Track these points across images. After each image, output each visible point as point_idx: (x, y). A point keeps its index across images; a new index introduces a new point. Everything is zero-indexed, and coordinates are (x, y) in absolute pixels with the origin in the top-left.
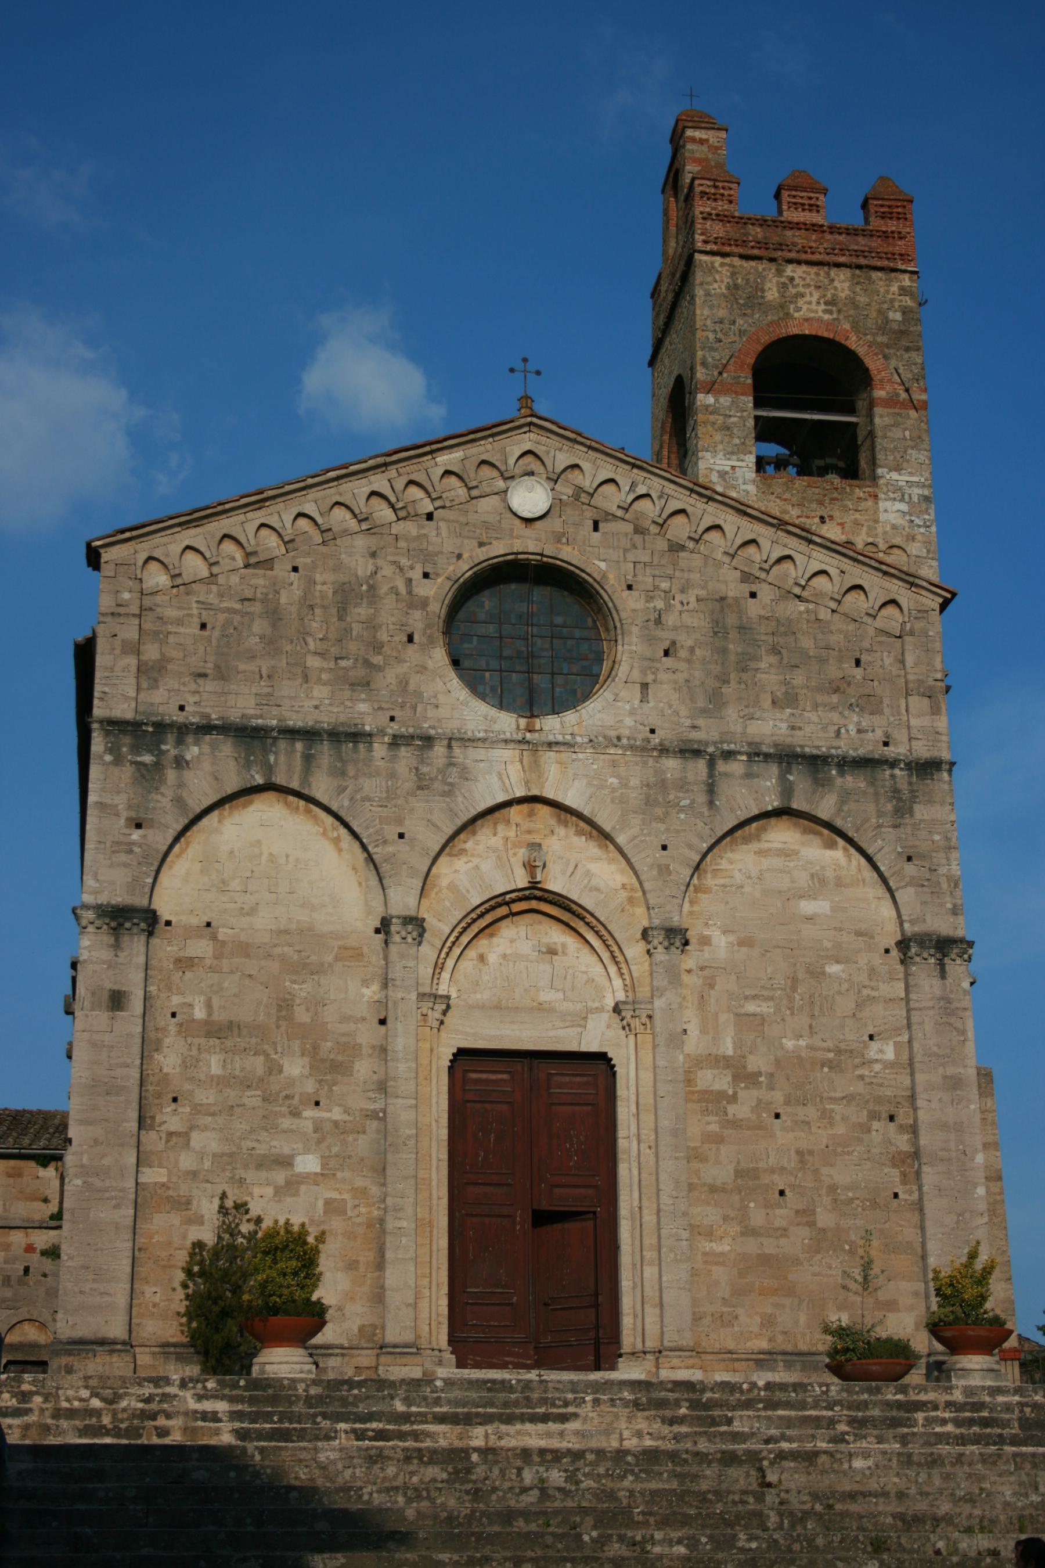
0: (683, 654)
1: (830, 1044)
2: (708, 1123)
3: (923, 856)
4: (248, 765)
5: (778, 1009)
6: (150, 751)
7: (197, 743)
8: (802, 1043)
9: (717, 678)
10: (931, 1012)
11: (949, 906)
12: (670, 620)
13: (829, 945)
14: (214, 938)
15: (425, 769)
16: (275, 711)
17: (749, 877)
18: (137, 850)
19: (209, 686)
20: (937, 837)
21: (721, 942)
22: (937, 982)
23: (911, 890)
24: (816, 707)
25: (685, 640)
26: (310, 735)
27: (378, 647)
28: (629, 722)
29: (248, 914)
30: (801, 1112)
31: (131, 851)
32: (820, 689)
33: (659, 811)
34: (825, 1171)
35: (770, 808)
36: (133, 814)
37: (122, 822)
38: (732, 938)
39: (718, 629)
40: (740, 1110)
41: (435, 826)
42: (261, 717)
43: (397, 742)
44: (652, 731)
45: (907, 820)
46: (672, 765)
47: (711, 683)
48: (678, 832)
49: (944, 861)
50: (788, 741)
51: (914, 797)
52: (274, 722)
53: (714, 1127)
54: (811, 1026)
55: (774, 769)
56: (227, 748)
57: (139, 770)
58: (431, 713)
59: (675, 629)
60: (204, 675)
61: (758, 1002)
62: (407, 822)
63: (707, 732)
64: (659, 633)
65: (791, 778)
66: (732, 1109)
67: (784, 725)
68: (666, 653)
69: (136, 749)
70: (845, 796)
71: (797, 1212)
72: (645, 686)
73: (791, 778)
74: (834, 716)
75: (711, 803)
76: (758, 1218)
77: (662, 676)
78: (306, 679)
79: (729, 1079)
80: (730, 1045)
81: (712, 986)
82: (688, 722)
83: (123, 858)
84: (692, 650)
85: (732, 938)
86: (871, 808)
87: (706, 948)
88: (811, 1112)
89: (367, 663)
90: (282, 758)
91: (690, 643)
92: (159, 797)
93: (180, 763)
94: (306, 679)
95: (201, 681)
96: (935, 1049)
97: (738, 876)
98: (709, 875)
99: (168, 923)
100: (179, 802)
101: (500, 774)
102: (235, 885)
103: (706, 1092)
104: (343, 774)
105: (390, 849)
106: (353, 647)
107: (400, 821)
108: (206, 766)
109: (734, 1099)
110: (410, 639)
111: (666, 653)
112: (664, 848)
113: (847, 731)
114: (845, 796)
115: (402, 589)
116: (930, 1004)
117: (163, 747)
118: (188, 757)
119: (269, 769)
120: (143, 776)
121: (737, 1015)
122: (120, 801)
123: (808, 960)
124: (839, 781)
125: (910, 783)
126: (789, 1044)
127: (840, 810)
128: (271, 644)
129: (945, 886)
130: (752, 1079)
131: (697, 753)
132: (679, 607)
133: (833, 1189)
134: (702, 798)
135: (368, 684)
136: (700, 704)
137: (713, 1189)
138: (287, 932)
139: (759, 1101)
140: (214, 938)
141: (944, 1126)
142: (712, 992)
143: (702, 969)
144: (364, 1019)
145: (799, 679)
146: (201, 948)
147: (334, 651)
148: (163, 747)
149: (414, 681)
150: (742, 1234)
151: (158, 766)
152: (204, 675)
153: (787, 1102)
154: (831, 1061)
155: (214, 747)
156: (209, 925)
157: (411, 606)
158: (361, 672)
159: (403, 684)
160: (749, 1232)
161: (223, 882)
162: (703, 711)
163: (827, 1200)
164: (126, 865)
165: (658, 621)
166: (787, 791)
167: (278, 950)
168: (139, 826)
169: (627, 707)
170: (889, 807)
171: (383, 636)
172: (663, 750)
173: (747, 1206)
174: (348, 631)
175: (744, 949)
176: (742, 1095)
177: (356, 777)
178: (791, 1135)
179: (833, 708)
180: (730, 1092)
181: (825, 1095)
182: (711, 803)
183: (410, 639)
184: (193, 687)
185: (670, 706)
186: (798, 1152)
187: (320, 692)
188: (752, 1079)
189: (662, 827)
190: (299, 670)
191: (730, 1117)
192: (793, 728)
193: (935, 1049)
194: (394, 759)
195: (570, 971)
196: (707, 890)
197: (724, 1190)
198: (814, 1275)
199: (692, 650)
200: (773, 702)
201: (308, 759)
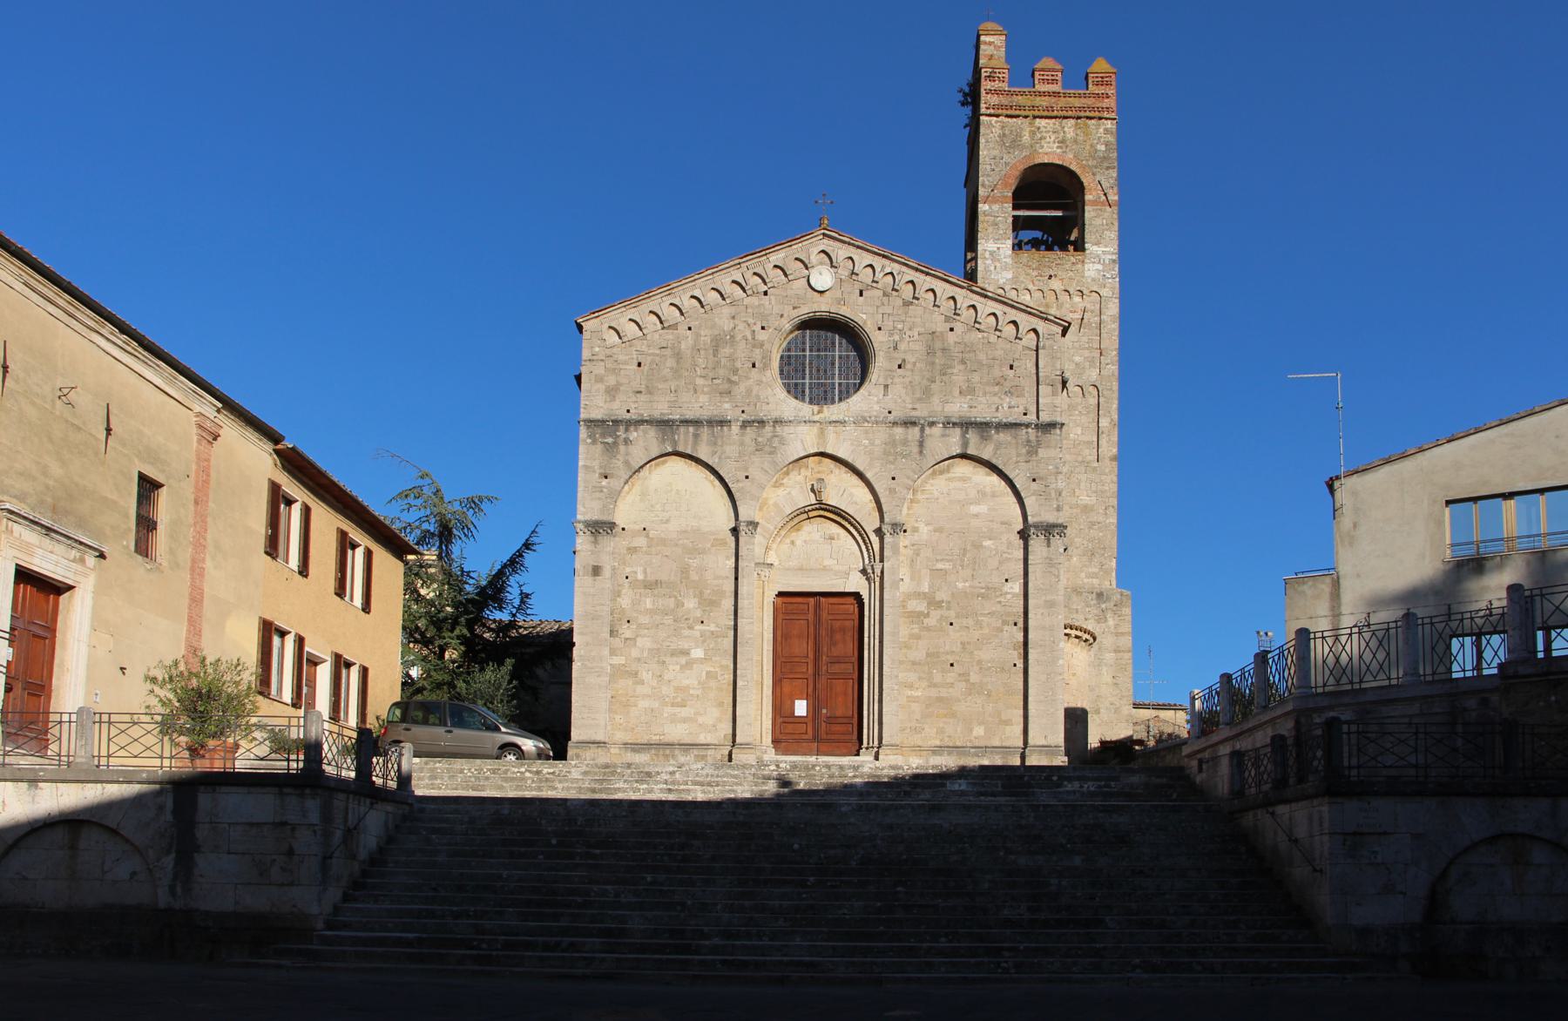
0: (908, 366)
1: (983, 585)
2: (912, 629)
3: (1041, 479)
4: (663, 441)
5: (954, 567)
6: (611, 436)
7: (636, 430)
8: (967, 584)
9: (928, 379)
10: (1040, 566)
11: (1055, 506)
12: (902, 347)
13: (986, 530)
14: (647, 536)
15: (760, 439)
16: (679, 410)
17: (943, 494)
18: (605, 490)
19: (642, 398)
20: (1051, 467)
21: (924, 529)
22: (1045, 549)
23: (1034, 498)
24: (985, 394)
25: (910, 359)
26: (696, 423)
27: (735, 371)
28: (876, 407)
29: (666, 523)
30: (964, 622)
31: (602, 491)
32: (988, 384)
33: (891, 458)
34: (976, 652)
35: (955, 454)
36: (602, 471)
37: (597, 475)
38: (930, 528)
39: (930, 352)
40: (931, 621)
41: (766, 471)
42: (671, 414)
43: (745, 424)
44: (890, 412)
45: (1034, 458)
46: (899, 431)
47: (925, 382)
48: (901, 469)
49: (1054, 481)
50: (968, 414)
51: (1039, 443)
52: (678, 417)
53: (916, 631)
54: (973, 575)
55: (958, 431)
56: (652, 432)
57: (605, 447)
58: (765, 407)
59: (905, 352)
60: (640, 392)
61: (943, 563)
62: (750, 469)
63: (921, 412)
64: (896, 355)
65: (968, 436)
66: (926, 621)
67: (966, 406)
68: (900, 367)
69: (603, 435)
70: (998, 446)
71: (960, 675)
72: (886, 386)
73: (968, 436)
74: (996, 399)
75: (921, 452)
76: (938, 678)
77: (896, 380)
78: (695, 391)
79: (926, 605)
80: (927, 587)
81: (918, 555)
82: (910, 406)
83: (598, 495)
84: (914, 364)
85: (930, 528)
86: (1014, 452)
87: (916, 534)
88: (970, 622)
89: (729, 381)
90: (682, 437)
91: (914, 360)
92: (616, 461)
93: (627, 441)
94: (695, 391)
95: (638, 395)
96: (1041, 586)
97: (936, 493)
98: (919, 493)
99: (623, 529)
100: (627, 463)
101: (802, 441)
102: (658, 507)
103: (912, 612)
104: (715, 444)
105: (740, 485)
106: (722, 372)
107: (746, 469)
108: (641, 443)
109: (927, 615)
110: (754, 366)
111: (900, 367)
112: (893, 478)
113: (1003, 407)
114: (998, 446)
115: (750, 337)
116: (1041, 561)
117: (618, 433)
118: (631, 439)
119: (675, 443)
120: (607, 450)
121: (930, 570)
122: (596, 464)
123: (972, 539)
124: (996, 436)
125: (1037, 437)
126: (960, 585)
127: (995, 453)
128: (676, 372)
129: (1053, 495)
130: (938, 605)
131: (914, 424)
132: (908, 339)
133: (979, 662)
134: (915, 449)
135: (730, 392)
136: (918, 395)
137: (914, 663)
138: (686, 532)
139: (942, 616)
140: (647, 536)
141: (1044, 628)
142: (918, 558)
143: (913, 545)
144: (727, 577)
145: (976, 378)
146: (641, 541)
147: (711, 375)
148: (618, 433)
149: (755, 389)
150: (929, 686)
151: (615, 444)
152: (640, 392)
153: (957, 617)
154: (983, 594)
155: (645, 432)
156: (644, 529)
157: (754, 346)
158: (727, 386)
159: (749, 391)
160: (933, 685)
161: (652, 506)
162: (920, 399)
163: (976, 668)
164: (599, 499)
165: (895, 348)
166: (965, 444)
167: (681, 542)
168: (606, 477)
169: (876, 399)
170: (1024, 451)
171: (738, 365)
172: (895, 423)
173: (932, 673)
174: (718, 362)
175: (937, 534)
176: (933, 613)
177: (722, 446)
178: (958, 634)
179: (995, 394)
180: (926, 612)
181: (979, 613)
182: (921, 452)
183: (754, 366)
184: (634, 399)
185: (901, 397)
186: (961, 643)
187: (703, 399)
188: (938, 605)
189: (893, 467)
190: (691, 387)
191: (925, 625)
192: (971, 407)
193: (1041, 586)
194: (743, 435)
195: (842, 549)
196: (918, 502)
197: (920, 664)
198: (967, 707)
199: (914, 364)
200: (960, 392)
201: (696, 436)
